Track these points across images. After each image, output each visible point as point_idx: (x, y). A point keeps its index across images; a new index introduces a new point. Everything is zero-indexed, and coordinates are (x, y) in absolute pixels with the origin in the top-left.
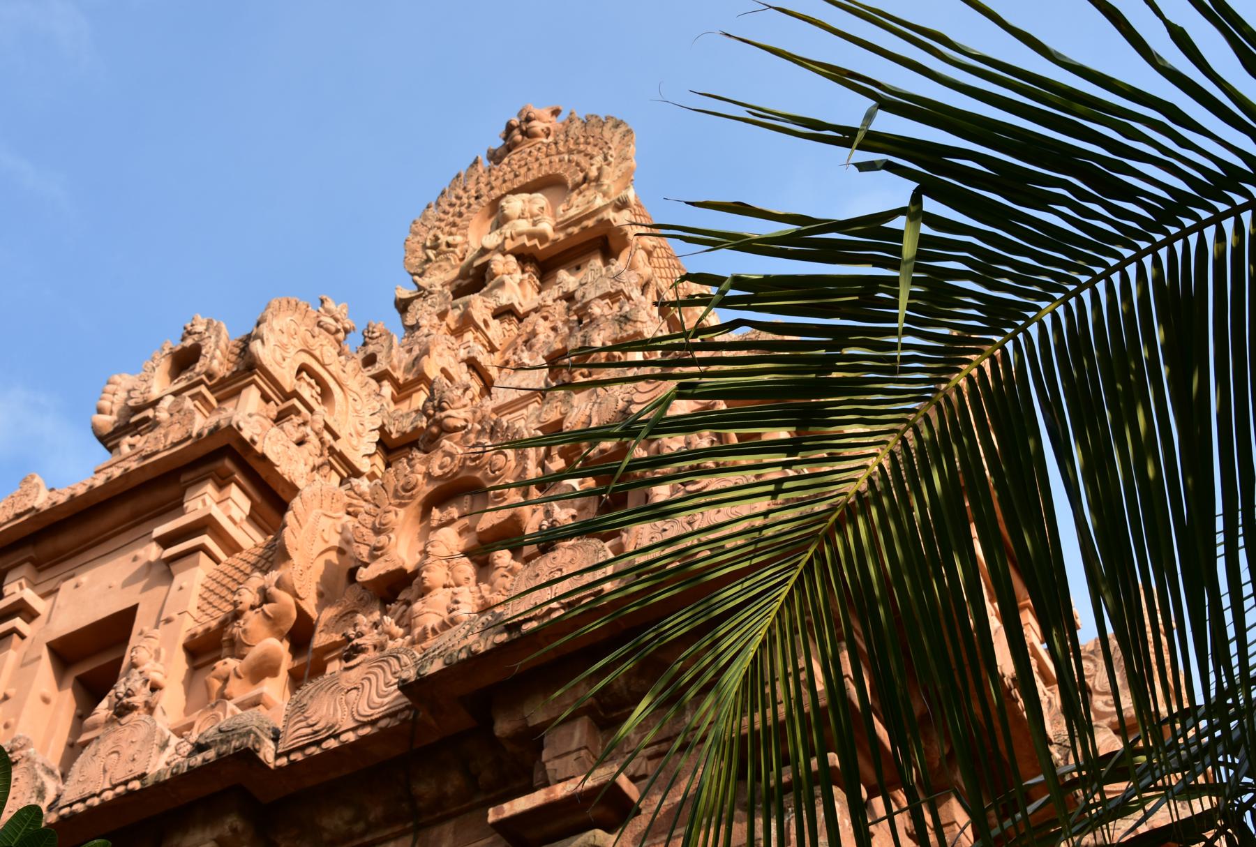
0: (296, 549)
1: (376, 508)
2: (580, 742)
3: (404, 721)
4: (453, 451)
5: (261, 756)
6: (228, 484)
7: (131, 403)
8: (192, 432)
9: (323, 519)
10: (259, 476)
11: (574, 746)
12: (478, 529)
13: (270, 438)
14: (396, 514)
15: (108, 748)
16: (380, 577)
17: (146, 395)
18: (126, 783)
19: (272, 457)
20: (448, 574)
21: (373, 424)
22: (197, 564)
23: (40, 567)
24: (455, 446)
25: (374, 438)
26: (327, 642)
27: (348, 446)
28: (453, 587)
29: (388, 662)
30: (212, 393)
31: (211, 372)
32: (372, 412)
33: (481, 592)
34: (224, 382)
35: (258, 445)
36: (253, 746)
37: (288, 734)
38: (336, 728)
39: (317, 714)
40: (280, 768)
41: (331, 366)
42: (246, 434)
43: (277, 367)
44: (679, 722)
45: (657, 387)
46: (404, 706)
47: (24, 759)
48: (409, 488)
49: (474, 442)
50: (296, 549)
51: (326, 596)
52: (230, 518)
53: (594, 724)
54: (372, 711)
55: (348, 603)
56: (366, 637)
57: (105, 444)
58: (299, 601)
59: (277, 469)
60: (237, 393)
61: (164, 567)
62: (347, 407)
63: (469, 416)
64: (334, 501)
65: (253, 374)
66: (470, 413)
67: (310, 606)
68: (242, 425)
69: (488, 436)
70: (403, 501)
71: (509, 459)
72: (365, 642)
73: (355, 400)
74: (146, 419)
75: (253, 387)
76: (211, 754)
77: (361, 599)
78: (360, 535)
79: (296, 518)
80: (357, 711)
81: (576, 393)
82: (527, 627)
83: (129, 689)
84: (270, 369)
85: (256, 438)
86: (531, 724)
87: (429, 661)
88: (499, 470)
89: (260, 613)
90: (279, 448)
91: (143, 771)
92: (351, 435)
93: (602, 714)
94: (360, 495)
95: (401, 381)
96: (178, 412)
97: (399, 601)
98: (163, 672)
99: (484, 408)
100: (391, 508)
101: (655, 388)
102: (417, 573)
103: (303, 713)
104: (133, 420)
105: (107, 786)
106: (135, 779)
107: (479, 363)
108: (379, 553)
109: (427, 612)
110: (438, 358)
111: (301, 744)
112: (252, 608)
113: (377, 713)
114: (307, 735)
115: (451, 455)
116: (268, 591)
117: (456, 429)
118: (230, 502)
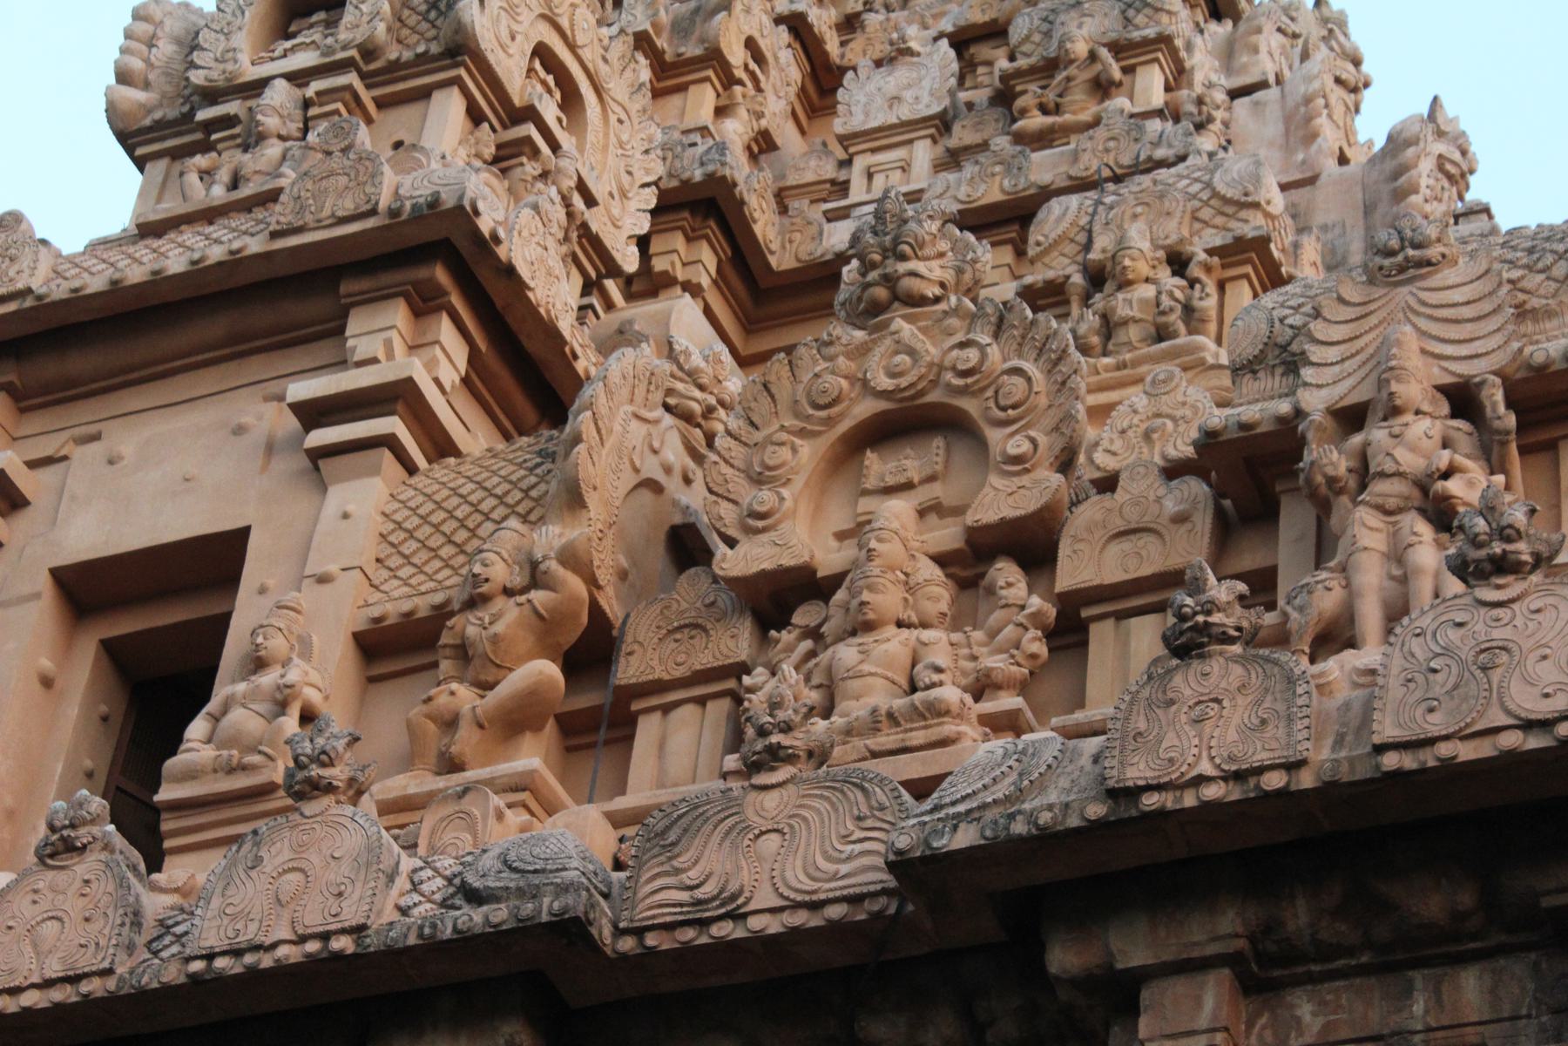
0: (595, 488)
1: (751, 429)
2: (1215, 1017)
3: (877, 916)
4: (918, 346)
5: (594, 931)
6: (437, 309)
7: (197, 77)
8: (377, 203)
9: (635, 424)
10: (493, 304)
11: (1203, 1021)
12: (971, 518)
13: (520, 233)
14: (794, 450)
15: (281, 859)
16: (763, 574)
17: (230, 67)
18: (325, 937)
19: (524, 271)
20: (906, 600)
21: (648, 172)
22: (375, 471)
23: (24, 404)
24: (921, 336)
25: (647, 202)
26: (644, 679)
27: (606, 219)
28: (916, 628)
29: (842, 792)
30: (368, 87)
31: (370, 46)
32: (647, 147)
33: (969, 646)
34: (395, 70)
35: (501, 247)
36: (586, 913)
37: (640, 895)
38: (740, 901)
39: (699, 868)
40: (624, 957)
41: (585, 49)
42: (485, 225)
43: (501, 54)
44: (1400, 1010)
45: (1362, 317)
46: (879, 887)
47: (99, 845)
48: (822, 401)
49: (960, 337)
50: (595, 488)
51: (630, 577)
52: (437, 381)
53: (1237, 984)
54: (816, 885)
55: (684, 605)
56: (796, 734)
57: (130, 150)
58: (595, 591)
59: (530, 295)
60: (424, 94)
61: (305, 462)
62: (606, 135)
63: (949, 276)
64: (652, 388)
65: (456, 65)
66: (952, 272)
67: (612, 605)
68: (481, 206)
69: (991, 328)
70: (809, 427)
71: (1036, 389)
72: (796, 743)
73: (620, 121)
74: (228, 121)
75: (455, 91)
76: (499, 914)
77: (713, 604)
78: (720, 479)
79: (596, 424)
80: (784, 879)
81: (1034, 150)
82: (1151, 801)
83: (324, 752)
84: (491, 58)
85: (502, 233)
86: (1120, 966)
87: (950, 824)
88: (1014, 407)
89: (527, 606)
90: (533, 252)
91: (363, 921)
92: (611, 195)
93: (1255, 968)
94: (690, 374)
95: (669, 57)
96: (343, 151)
97: (796, 626)
98: (321, 686)
99: (978, 266)
100: (784, 436)
101: (1357, 319)
102: (836, 581)
103: (670, 859)
104: (202, 115)
105: (286, 934)
106: (343, 931)
107: (810, 27)
108: (760, 524)
109: (871, 674)
110: (742, 16)
111: (668, 919)
112: (508, 592)
113: (826, 890)
114: (681, 905)
115: (911, 352)
116: (543, 567)
117: (922, 301)
118: (438, 351)
